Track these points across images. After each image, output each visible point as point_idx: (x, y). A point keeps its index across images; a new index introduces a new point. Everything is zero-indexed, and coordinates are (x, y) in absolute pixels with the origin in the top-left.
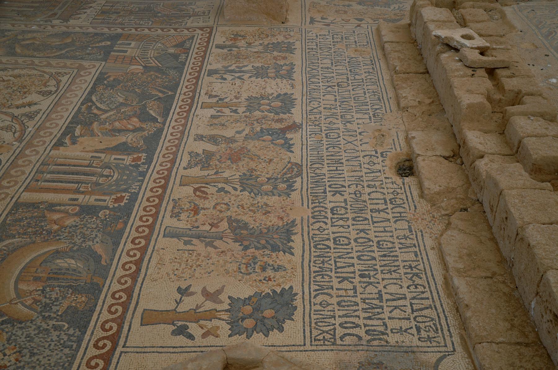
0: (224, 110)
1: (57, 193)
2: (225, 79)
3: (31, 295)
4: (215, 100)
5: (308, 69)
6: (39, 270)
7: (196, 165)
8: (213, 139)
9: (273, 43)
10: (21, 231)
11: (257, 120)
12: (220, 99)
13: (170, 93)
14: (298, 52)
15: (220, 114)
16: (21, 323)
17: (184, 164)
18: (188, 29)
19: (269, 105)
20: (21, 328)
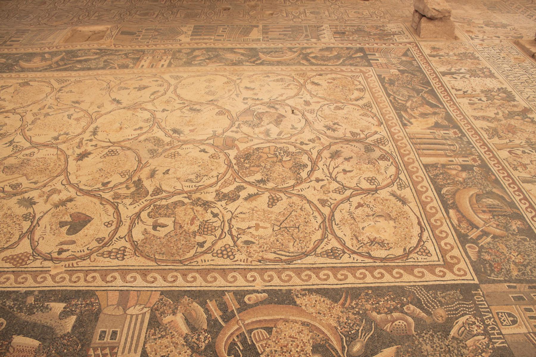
0: (473, 99)
1: (437, 157)
2: (456, 78)
3: (490, 222)
4: (461, 92)
5: (501, 72)
6: (480, 206)
7: (493, 136)
8: (484, 118)
9: (461, 54)
10: (445, 182)
11: (500, 106)
12: (464, 92)
13: (429, 88)
14: (481, 58)
15: (471, 102)
16: (503, 238)
17: (486, 136)
18: (401, 44)
19: (498, 95)
20: (506, 241)
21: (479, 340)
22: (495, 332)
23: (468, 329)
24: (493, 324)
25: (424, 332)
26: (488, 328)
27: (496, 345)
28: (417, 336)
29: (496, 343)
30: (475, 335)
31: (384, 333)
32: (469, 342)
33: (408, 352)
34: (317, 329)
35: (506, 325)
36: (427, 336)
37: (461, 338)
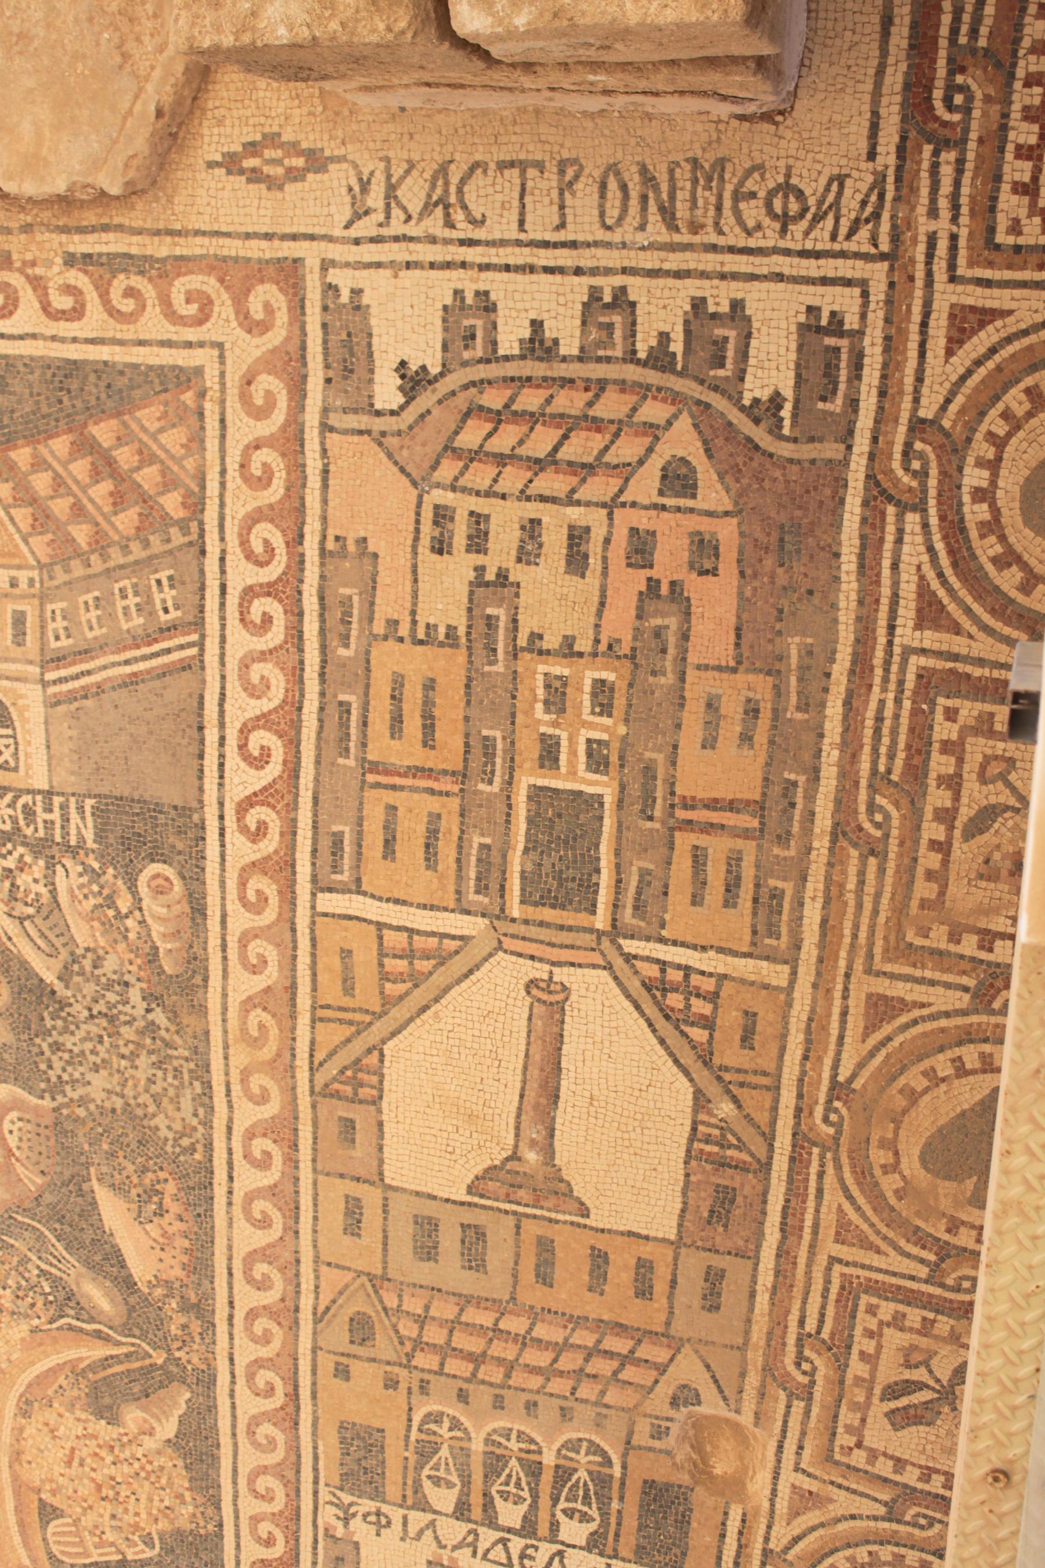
21: (71, 891)
22: (41, 816)
23: (31, 911)
24: (12, 805)
25: (43, 1066)
26: (29, 831)
27: (89, 835)
28: (60, 1098)
29: (82, 839)
30: (53, 893)
31: (48, 1198)
32: (82, 934)
33: (113, 1155)
34: (40, 1380)
35: (16, 754)
36: (57, 1065)
37: (64, 955)
